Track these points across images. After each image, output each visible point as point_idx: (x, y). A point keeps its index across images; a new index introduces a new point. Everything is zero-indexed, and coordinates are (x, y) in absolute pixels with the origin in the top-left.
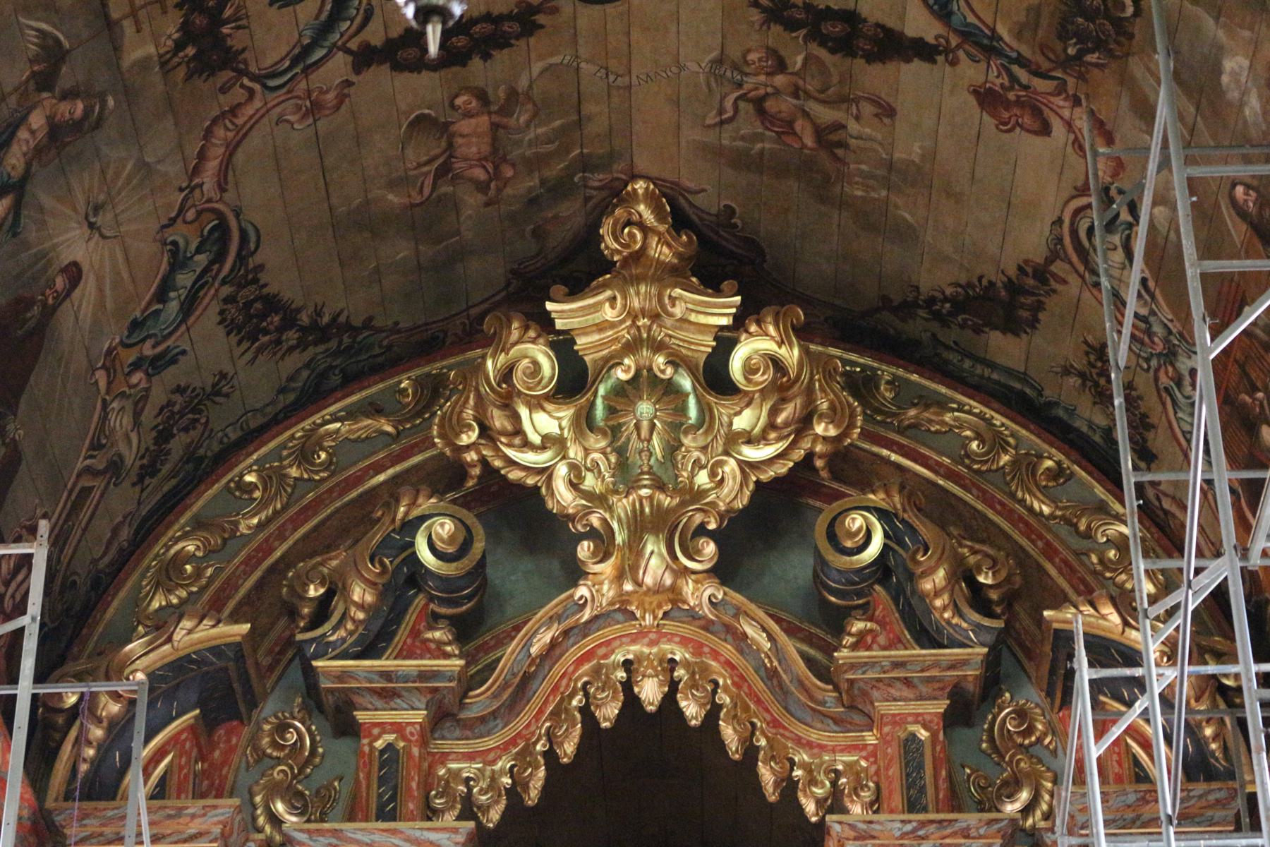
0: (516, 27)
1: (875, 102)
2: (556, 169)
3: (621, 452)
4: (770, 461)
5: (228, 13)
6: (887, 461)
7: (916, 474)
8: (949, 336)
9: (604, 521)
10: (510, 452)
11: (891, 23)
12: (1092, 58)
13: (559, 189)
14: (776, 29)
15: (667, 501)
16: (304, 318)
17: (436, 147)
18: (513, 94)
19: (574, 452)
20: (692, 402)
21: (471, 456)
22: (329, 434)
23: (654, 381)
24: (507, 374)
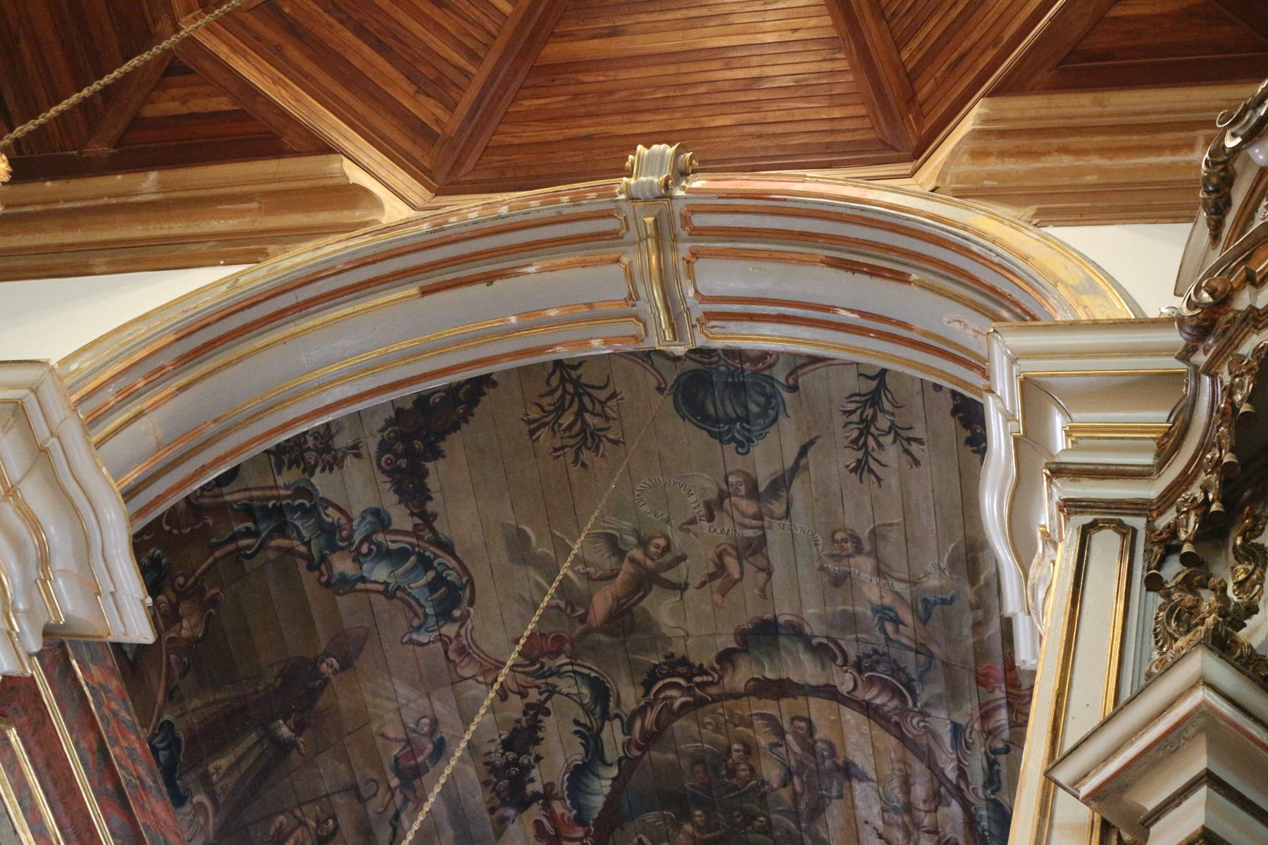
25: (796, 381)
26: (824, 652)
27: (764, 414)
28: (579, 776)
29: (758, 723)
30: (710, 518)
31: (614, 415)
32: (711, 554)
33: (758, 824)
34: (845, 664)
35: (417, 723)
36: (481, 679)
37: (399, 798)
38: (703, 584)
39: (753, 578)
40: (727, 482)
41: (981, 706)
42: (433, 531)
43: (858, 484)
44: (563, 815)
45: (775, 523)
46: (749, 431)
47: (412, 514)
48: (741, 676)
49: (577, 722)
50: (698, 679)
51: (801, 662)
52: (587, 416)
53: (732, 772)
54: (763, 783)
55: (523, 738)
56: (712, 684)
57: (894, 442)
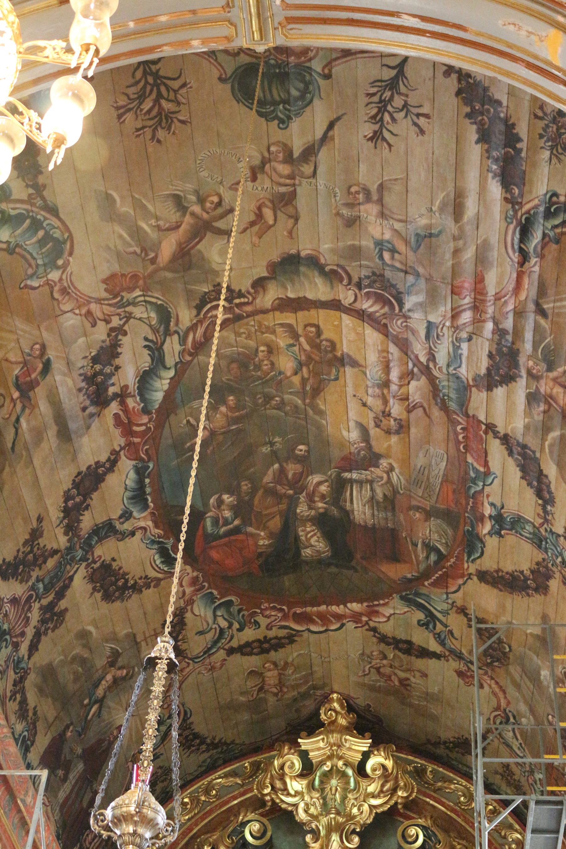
0: (287, 641)
1: (419, 671)
2: (303, 689)
3: (324, 799)
4: (381, 805)
5: (180, 637)
6: (428, 803)
7: (440, 810)
8: (453, 755)
9: (317, 826)
10: (283, 798)
11: (424, 646)
12: (496, 664)
13: (305, 696)
14: (382, 645)
15: (341, 820)
16: (208, 741)
17: (258, 681)
18: (286, 664)
19: (307, 798)
20: (352, 780)
21: (268, 798)
22: (217, 783)
23: (338, 771)
24: (282, 767)
25: (330, 71)
26: (332, 276)
27: (302, 97)
28: (145, 379)
29: (279, 330)
30: (254, 179)
31: (184, 101)
32: (253, 206)
33: (274, 402)
34: (349, 284)
35: (32, 348)
36: (77, 311)
37: (19, 406)
38: (245, 230)
39: (284, 223)
40: (269, 151)
41: (452, 310)
42: (43, 198)
43: (373, 150)
44: (134, 408)
45: (304, 181)
46: (289, 110)
47: (27, 186)
48: (271, 295)
49: (146, 339)
50: (237, 301)
51: (316, 284)
52: (163, 102)
53: (258, 367)
54: (280, 373)
55: (108, 354)
56: (247, 304)
57: (406, 116)
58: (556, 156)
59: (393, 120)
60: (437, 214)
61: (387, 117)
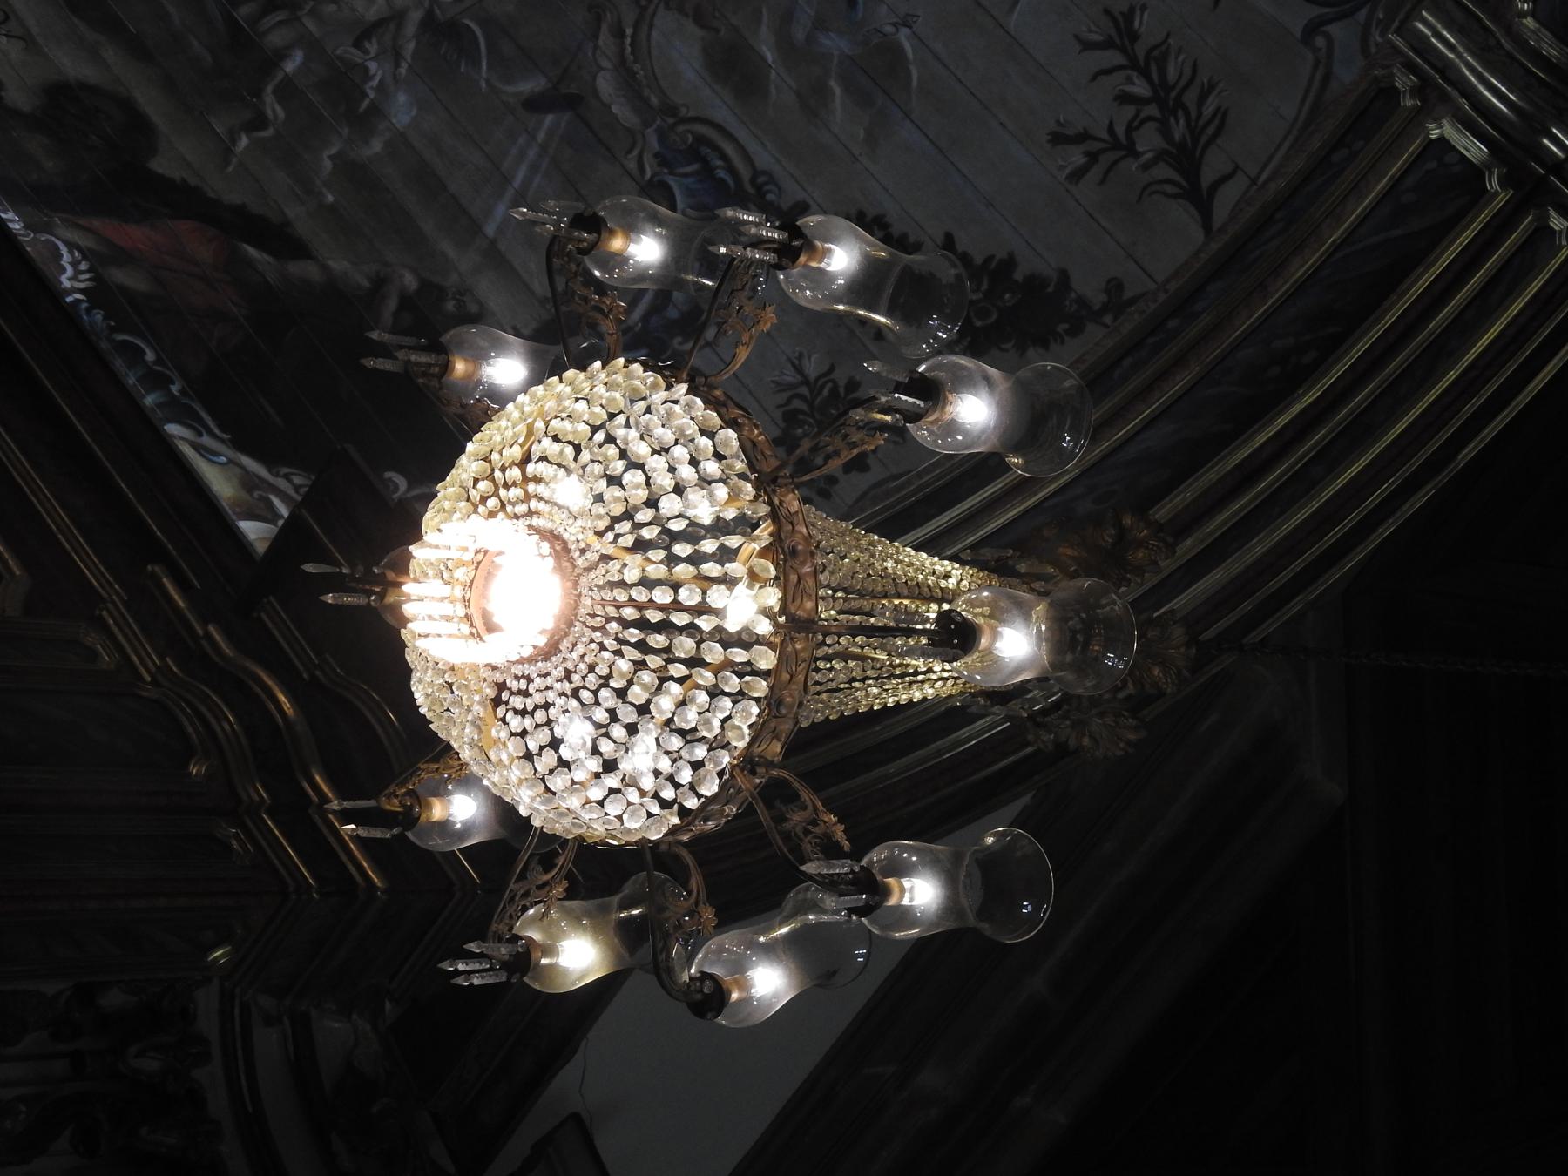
58: (791, 386)
59: (1124, 98)
60: (889, 29)
61: (1140, 88)
